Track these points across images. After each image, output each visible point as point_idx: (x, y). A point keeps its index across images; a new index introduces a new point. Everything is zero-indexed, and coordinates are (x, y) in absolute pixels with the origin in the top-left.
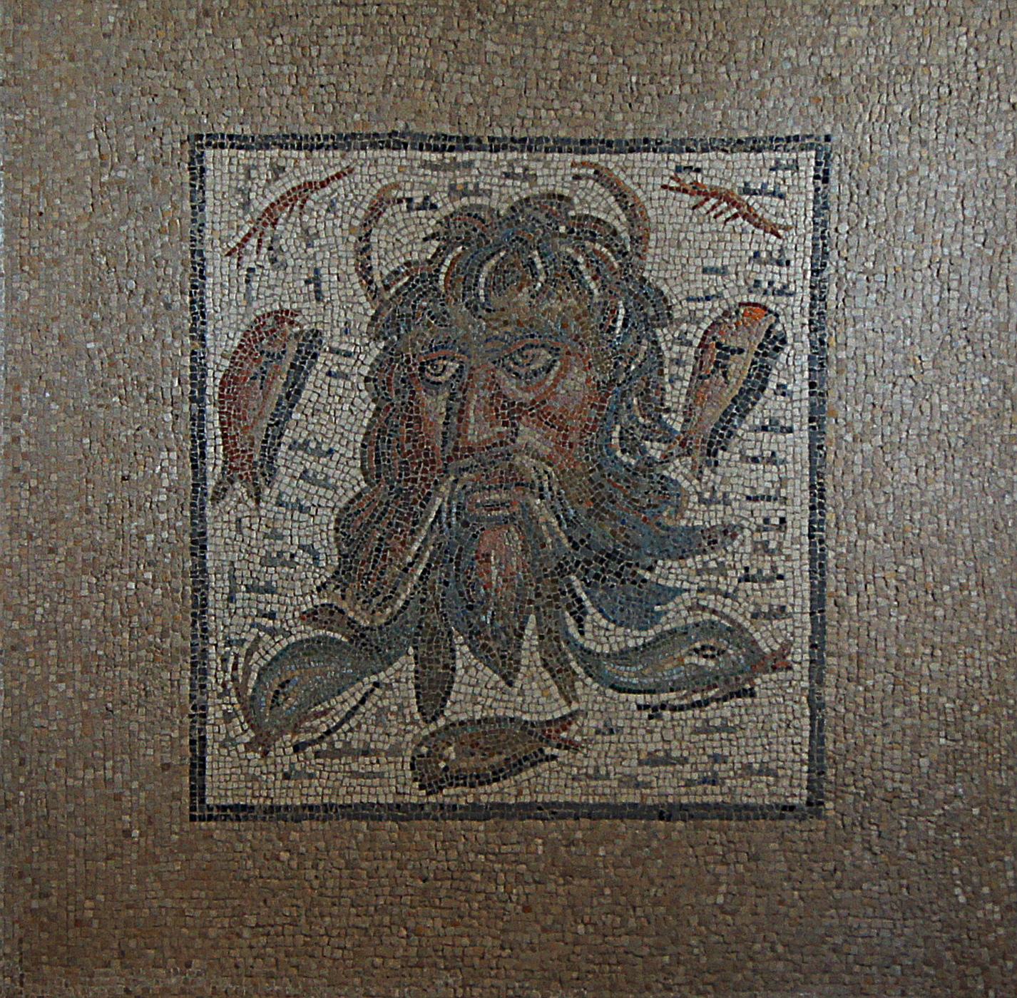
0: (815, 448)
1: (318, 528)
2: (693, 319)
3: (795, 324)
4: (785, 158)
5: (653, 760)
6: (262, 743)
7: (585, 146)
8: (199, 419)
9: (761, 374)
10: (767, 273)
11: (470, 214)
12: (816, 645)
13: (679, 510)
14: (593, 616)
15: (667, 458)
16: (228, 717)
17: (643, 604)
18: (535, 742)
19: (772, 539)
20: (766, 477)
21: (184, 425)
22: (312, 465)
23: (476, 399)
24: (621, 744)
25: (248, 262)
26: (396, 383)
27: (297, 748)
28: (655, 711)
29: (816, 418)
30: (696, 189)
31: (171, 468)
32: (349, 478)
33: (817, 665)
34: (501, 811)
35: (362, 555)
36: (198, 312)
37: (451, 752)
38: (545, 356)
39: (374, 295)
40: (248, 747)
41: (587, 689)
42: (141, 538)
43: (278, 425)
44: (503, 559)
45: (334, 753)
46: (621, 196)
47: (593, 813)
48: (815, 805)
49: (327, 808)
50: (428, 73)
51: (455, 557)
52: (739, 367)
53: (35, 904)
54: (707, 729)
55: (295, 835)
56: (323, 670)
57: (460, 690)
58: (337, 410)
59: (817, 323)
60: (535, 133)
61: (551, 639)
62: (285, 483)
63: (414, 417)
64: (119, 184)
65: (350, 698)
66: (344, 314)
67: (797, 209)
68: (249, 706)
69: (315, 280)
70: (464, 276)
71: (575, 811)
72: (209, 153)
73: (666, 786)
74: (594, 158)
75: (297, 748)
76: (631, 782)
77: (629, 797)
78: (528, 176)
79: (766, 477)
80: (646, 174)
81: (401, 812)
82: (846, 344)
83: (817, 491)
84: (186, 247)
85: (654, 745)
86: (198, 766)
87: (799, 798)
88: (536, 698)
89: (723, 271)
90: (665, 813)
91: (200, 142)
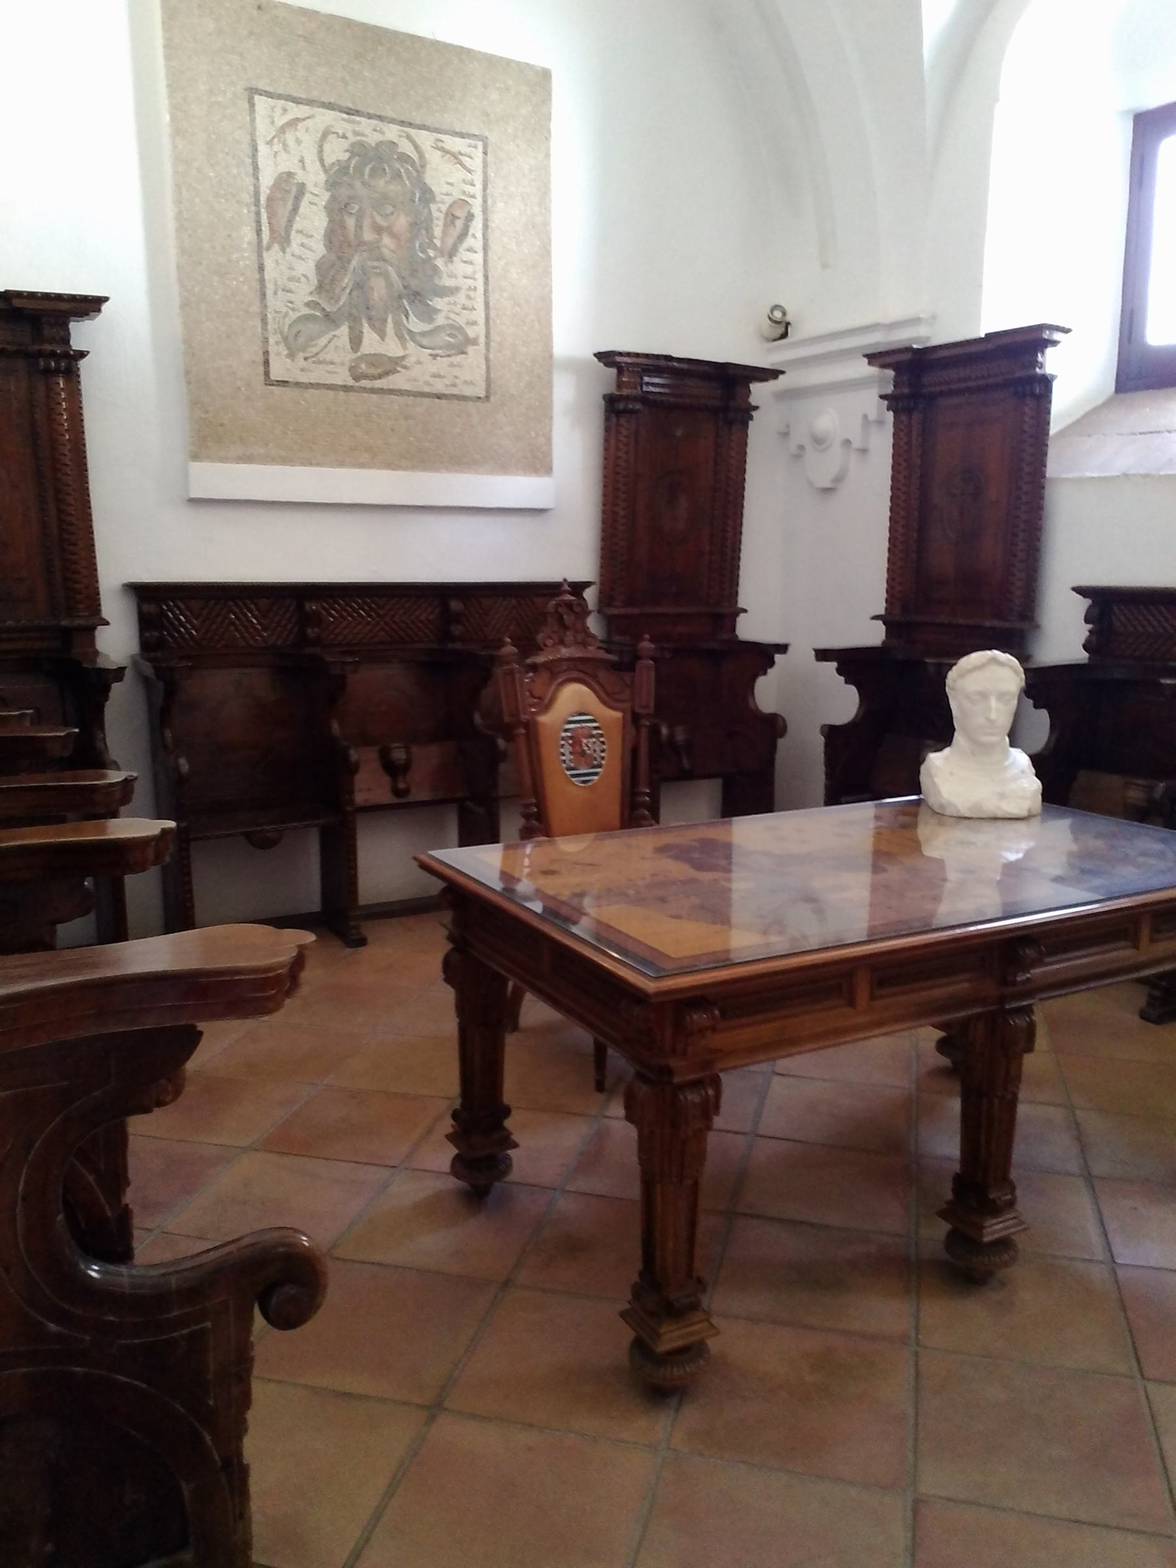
0: (485, 261)
1: (307, 268)
2: (443, 203)
4: (472, 142)
5: (434, 376)
8: (258, 214)
10: (468, 188)
11: (361, 144)
12: (487, 336)
13: (440, 278)
15: (435, 258)
16: (277, 343)
17: (428, 314)
18: (392, 365)
19: (472, 294)
20: (469, 269)
21: (252, 216)
22: (305, 241)
23: (366, 223)
24: (423, 369)
25: (276, 148)
26: (337, 210)
27: (306, 359)
28: (435, 356)
29: (486, 248)
30: (442, 149)
31: (248, 234)
32: (319, 248)
33: (488, 344)
34: (381, 391)
35: (326, 281)
37: (363, 366)
38: (390, 209)
39: (326, 171)
40: (287, 356)
41: (411, 345)
42: (237, 262)
43: (290, 221)
44: (379, 290)
45: (320, 362)
46: (416, 147)
48: (487, 397)
49: (318, 384)
50: (343, 80)
52: (459, 224)
53: (203, 416)
54: (452, 365)
55: (306, 395)
56: (314, 328)
57: (366, 341)
58: (313, 219)
59: (485, 211)
60: (383, 114)
61: (398, 325)
62: (295, 247)
63: (343, 227)
64: (219, 103)
65: (323, 341)
66: (314, 178)
67: (476, 163)
68: (285, 339)
69: (302, 161)
70: (359, 170)
72: (257, 97)
73: (439, 387)
74: (405, 129)
75: (306, 359)
76: (427, 383)
77: (427, 389)
78: (382, 132)
79: (469, 269)
80: (425, 139)
81: (346, 388)
82: (496, 220)
83: (486, 277)
84: (249, 137)
85: (434, 369)
86: (266, 363)
87: (482, 394)
88: (392, 348)
89: (451, 184)
90: (439, 397)
91: (253, 91)
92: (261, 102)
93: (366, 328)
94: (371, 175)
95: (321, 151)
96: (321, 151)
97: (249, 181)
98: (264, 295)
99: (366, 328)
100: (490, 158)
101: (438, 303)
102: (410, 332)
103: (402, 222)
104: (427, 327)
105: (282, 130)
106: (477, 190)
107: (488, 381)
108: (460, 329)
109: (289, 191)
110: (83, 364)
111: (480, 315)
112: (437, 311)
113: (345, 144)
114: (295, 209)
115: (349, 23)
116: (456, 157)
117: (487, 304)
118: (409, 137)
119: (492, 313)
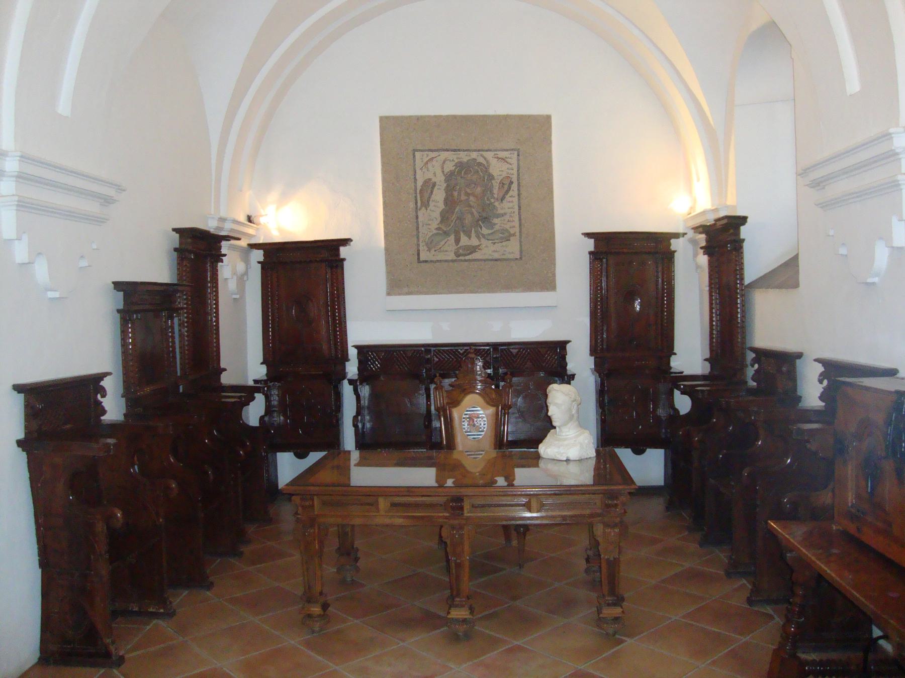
0: (519, 200)
1: (436, 215)
3: (514, 178)
5: (494, 251)
6: (429, 250)
7: (479, 151)
8: (416, 197)
9: (509, 188)
11: (461, 163)
14: (483, 228)
17: (492, 226)
18: (473, 249)
20: (511, 205)
24: (488, 250)
26: (449, 190)
31: (412, 205)
32: (442, 206)
36: (415, 179)
41: (483, 240)
43: (430, 197)
44: (468, 219)
46: (485, 159)
47: (485, 260)
48: (521, 258)
51: (460, 219)
58: (439, 196)
63: (452, 195)
65: (443, 243)
66: (440, 179)
67: (514, 161)
68: (427, 244)
69: (435, 174)
70: (459, 172)
71: (481, 260)
73: (496, 256)
79: (511, 205)
80: (489, 155)
81: (453, 261)
86: (418, 254)
88: (474, 242)
90: (496, 260)
91: (415, 151)
92: (418, 154)
93: (462, 234)
94: (465, 173)
95: (443, 168)
96: (443, 168)
97: (413, 185)
98: (418, 228)
99: (462, 234)
100: (521, 157)
101: (496, 221)
102: (484, 236)
103: (479, 190)
104: (490, 232)
105: (427, 163)
106: (515, 172)
107: (521, 252)
108: (507, 230)
109: (430, 185)
110: (345, 263)
111: (517, 224)
112: (495, 224)
113: (454, 163)
114: (432, 192)
115: (455, 117)
116: (504, 160)
117: (520, 220)
118: (482, 156)
119: (523, 222)
